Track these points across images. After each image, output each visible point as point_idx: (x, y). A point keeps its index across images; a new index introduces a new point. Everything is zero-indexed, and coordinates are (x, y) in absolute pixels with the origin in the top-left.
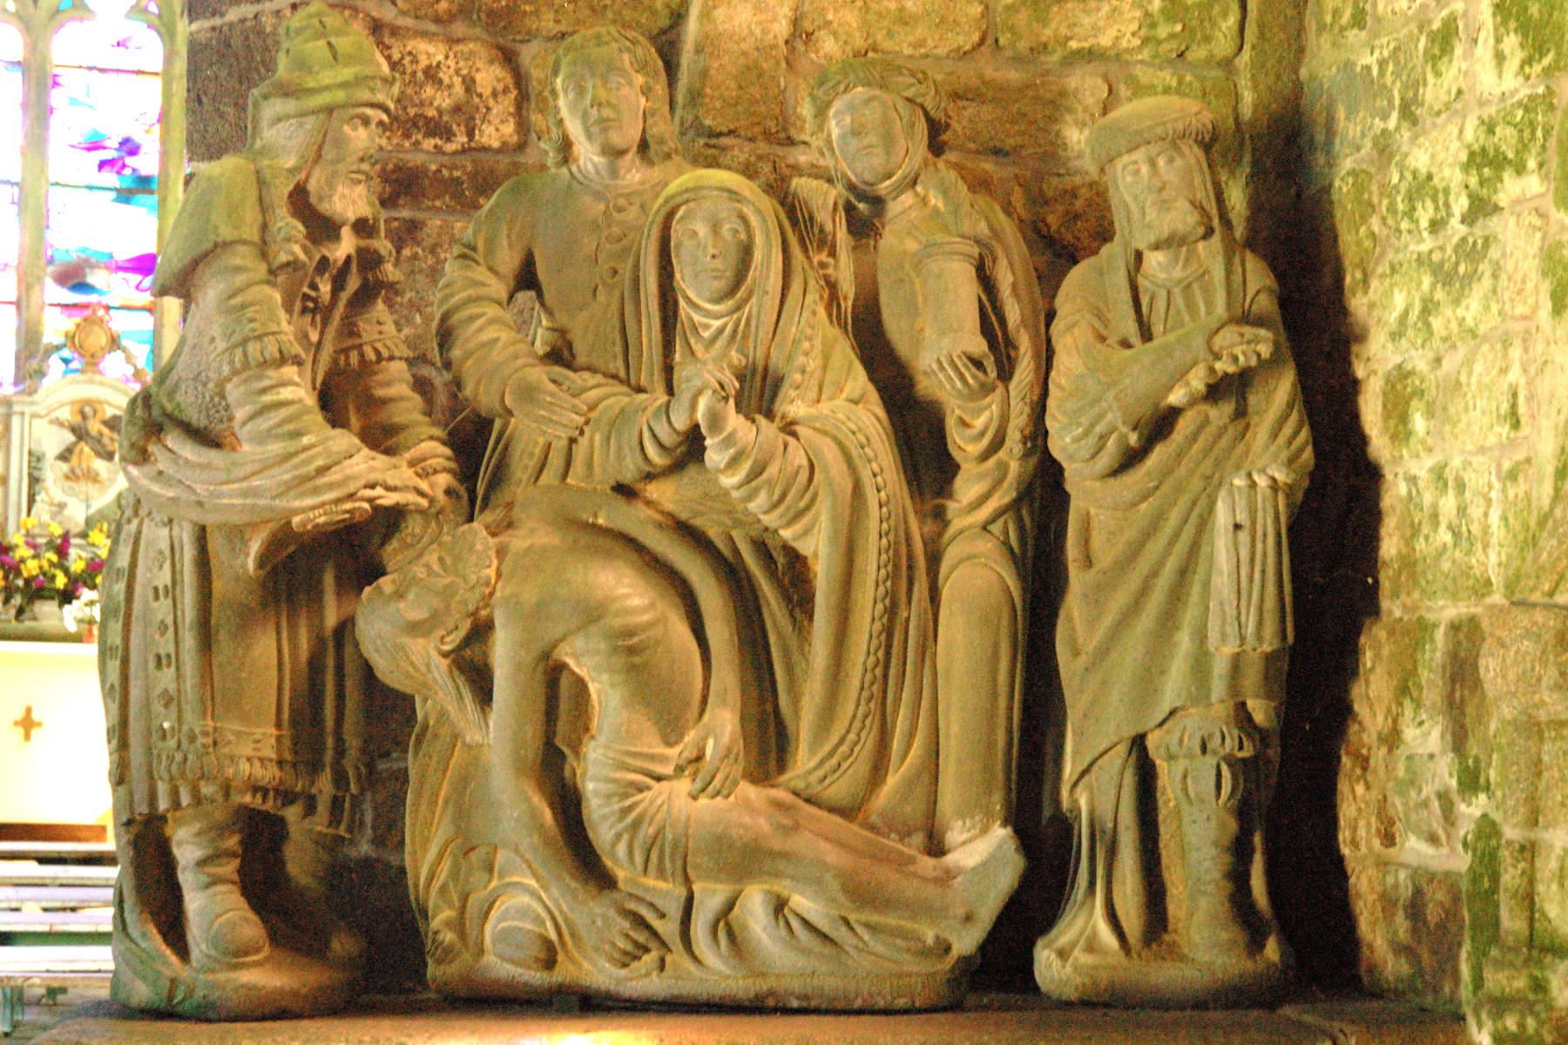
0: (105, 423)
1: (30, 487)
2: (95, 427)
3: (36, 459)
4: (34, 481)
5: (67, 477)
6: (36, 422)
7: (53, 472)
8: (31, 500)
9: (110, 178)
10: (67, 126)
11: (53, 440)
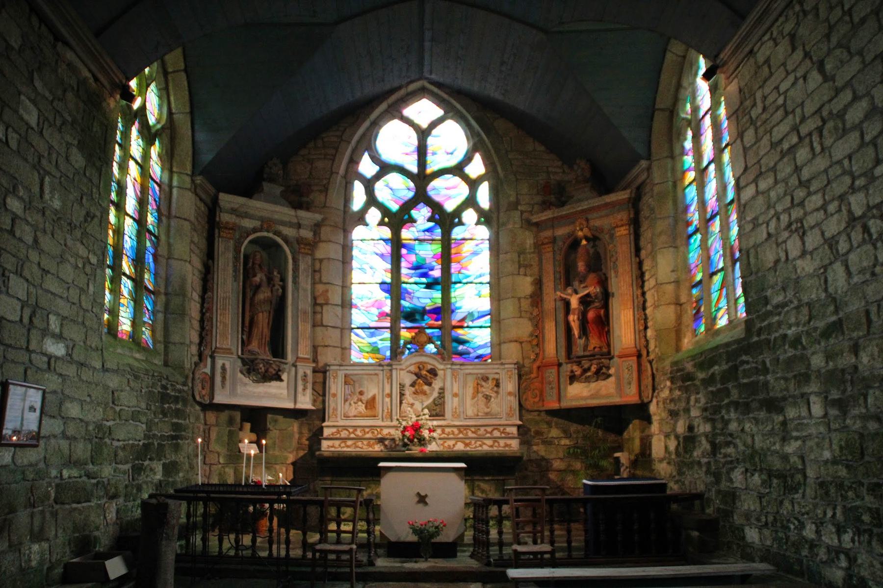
0: (428, 371)
1: (400, 397)
2: (424, 372)
3: (402, 386)
4: (402, 395)
5: (414, 393)
6: (402, 372)
7: (408, 391)
8: (401, 403)
9: (424, 280)
11: (408, 379)
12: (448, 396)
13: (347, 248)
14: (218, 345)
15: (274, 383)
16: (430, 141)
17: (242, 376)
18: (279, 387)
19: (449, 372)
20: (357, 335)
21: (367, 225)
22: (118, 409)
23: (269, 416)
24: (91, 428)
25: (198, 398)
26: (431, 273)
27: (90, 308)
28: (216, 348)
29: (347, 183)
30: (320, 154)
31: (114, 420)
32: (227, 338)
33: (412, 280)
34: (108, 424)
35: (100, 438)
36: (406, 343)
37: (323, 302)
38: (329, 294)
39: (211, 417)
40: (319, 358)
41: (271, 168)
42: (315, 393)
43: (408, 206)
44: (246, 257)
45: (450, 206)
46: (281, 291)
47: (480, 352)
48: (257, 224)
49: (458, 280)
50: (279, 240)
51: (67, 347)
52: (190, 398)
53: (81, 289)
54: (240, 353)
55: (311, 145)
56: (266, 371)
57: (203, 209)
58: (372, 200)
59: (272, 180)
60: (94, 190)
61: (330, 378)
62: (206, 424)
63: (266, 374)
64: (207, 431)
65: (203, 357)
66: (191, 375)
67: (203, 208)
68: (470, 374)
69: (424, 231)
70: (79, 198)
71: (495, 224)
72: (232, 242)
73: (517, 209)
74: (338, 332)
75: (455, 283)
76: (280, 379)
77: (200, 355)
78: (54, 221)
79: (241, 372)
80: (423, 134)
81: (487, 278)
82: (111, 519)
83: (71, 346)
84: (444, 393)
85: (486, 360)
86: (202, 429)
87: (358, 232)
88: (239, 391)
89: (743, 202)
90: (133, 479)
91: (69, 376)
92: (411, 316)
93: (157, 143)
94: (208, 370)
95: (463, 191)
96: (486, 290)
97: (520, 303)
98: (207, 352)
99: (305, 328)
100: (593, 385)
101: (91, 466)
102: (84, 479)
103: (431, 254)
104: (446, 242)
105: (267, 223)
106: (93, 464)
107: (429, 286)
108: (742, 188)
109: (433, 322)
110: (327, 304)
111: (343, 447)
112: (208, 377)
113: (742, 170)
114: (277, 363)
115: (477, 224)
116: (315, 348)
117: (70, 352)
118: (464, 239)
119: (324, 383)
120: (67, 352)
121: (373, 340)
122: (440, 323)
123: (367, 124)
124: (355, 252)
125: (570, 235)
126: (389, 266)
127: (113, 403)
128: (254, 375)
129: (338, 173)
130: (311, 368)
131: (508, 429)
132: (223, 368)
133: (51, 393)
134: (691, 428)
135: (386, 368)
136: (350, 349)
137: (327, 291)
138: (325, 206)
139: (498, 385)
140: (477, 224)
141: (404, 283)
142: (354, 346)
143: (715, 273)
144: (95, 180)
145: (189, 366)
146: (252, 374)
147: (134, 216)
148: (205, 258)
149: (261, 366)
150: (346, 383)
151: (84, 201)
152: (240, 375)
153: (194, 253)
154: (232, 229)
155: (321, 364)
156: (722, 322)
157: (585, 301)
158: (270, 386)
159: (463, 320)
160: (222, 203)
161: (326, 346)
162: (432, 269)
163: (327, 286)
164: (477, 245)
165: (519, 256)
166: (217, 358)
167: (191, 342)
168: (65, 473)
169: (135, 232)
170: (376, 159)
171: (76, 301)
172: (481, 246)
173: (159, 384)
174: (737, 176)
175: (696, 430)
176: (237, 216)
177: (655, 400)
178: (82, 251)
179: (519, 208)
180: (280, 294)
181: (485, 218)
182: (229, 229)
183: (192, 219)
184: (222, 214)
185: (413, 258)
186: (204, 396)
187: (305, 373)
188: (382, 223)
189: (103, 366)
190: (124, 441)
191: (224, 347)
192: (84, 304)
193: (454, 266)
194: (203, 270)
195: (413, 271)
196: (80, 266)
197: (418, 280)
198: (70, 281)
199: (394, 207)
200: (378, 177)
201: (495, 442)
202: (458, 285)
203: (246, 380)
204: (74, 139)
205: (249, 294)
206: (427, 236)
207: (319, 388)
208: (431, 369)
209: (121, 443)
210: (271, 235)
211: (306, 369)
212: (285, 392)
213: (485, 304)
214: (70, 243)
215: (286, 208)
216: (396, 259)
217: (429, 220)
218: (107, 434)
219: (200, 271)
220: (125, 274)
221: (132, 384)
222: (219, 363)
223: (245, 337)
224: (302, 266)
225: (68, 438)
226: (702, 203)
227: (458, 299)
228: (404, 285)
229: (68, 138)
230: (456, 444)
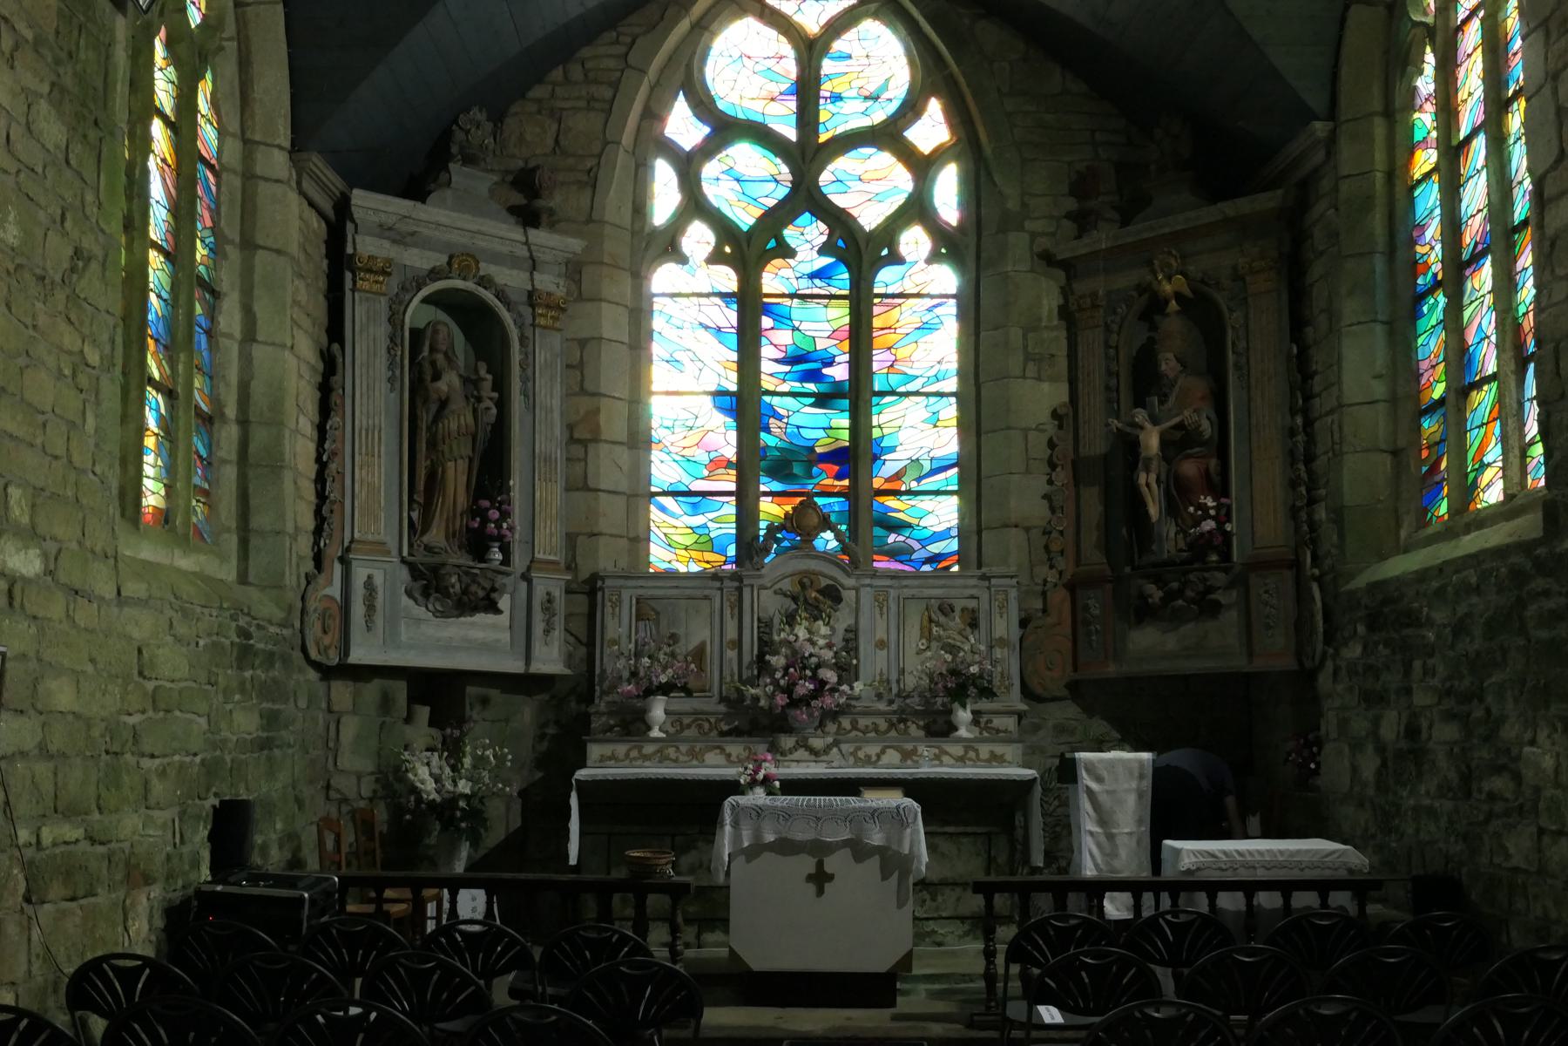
0: (819, 591)
6: (764, 592)
9: (811, 387)
10: (775, 342)
12: (865, 646)
13: (639, 315)
14: (357, 535)
15: (480, 618)
16: (827, 66)
17: (411, 603)
18: (494, 627)
19: (867, 596)
20: (663, 509)
21: (683, 260)
22: (150, 686)
23: (472, 691)
24: (96, 733)
25: (314, 654)
26: (826, 371)
27: (89, 466)
28: (352, 541)
29: (637, 166)
30: (579, 98)
31: (143, 712)
33: (785, 388)
34: (131, 720)
35: (116, 754)
36: (771, 529)
37: (588, 436)
38: (602, 418)
39: (342, 692)
40: (578, 559)
41: (467, 132)
42: (571, 639)
43: (776, 218)
44: (416, 334)
45: (870, 218)
46: (494, 411)
47: (935, 548)
48: (441, 260)
49: (888, 389)
50: (488, 296)
51: (45, 556)
52: (297, 655)
53: (72, 425)
54: (405, 553)
55: (557, 74)
56: (465, 591)
57: (316, 225)
58: (695, 204)
59: (469, 160)
60: (90, 198)
62: (330, 711)
63: (465, 598)
65: (326, 564)
66: (299, 605)
67: (317, 224)
68: (913, 597)
69: (812, 276)
70: (58, 219)
71: (972, 265)
72: (383, 300)
73: (1021, 228)
74: (620, 502)
75: (882, 394)
76: (492, 608)
77: (318, 559)
78: (8, 272)
79: (409, 594)
80: (811, 50)
81: (951, 385)
82: (138, 932)
83: (54, 552)
84: (856, 639)
85: (948, 568)
86: (321, 721)
87: (664, 277)
88: (404, 638)
89: (1550, 232)
90: (182, 841)
91: (50, 620)
92: (782, 467)
93: (209, 76)
94: (335, 591)
95: (902, 182)
96: (949, 410)
97: (1026, 438)
98: (333, 551)
99: (551, 495)
100: (1188, 629)
101: (96, 816)
102: (84, 846)
103: (827, 328)
104: (861, 302)
105: (462, 261)
106: (101, 813)
107: (822, 400)
108: (1551, 200)
109: (829, 482)
111: (635, 759)
113: (1551, 160)
114: (490, 574)
115: (929, 261)
116: (571, 539)
117: (52, 567)
118: (901, 295)
119: (591, 616)
120: (46, 566)
121: (698, 520)
122: (846, 482)
123: (684, 25)
124: (657, 323)
125: (1142, 289)
126: (734, 357)
127: (141, 673)
128: (437, 599)
129: (619, 143)
130: (563, 583)
131: (998, 722)
132: (369, 585)
133: (16, 658)
134: (1412, 732)
135: (727, 583)
136: (648, 540)
137: (597, 411)
138: (590, 220)
139: (974, 625)
140: (929, 261)
141: (768, 393)
142: (656, 534)
143: (1477, 386)
144: (90, 175)
145: (294, 583)
146: (432, 599)
147: (164, 244)
148: (324, 339)
149: (454, 579)
150: (639, 618)
151: (68, 224)
152: (405, 601)
153: (299, 327)
154: (384, 273)
155: (584, 574)
156: (1492, 493)
157: (1178, 442)
158: (473, 624)
159: (898, 476)
160: (357, 213)
161: (595, 535)
162: (830, 363)
164: (930, 310)
165: (1025, 337)
166: (354, 563)
167: (296, 528)
168: (47, 836)
169: (167, 285)
170: (704, 106)
171: (60, 450)
172: (938, 311)
173: (234, 624)
174: (1540, 171)
175: (1424, 735)
176: (394, 241)
177: (1329, 665)
178: (70, 340)
179: (1028, 225)
180: (493, 419)
181: (948, 245)
182: (376, 273)
183: (294, 249)
184: (359, 239)
185: (784, 337)
186: (327, 648)
187: (548, 594)
188: (716, 258)
189: (119, 593)
190: (165, 756)
191: (370, 537)
192: (76, 458)
193: (879, 360)
194: (320, 366)
195: (787, 368)
196: (67, 372)
197: (797, 386)
198: (49, 408)
199: (745, 218)
200: (708, 149)
201: (967, 749)
202: (888, 399)
203: (420, 611)
204: (42, 81)
205: (425, 419)
206: (819, 287)
207: (580, 628)
208: (828, 586)
209: (157, 761)
210: (469, 285)
211: (549, 585)
212: (505, 637)
213: (947, 443)
214: (42, 320)
215: (504, 226)
216: (748, 341)
217: (823, 250)
218: (130, 743)
219: (313, 368)
220: (151, 381)
221: (181, 630)
222: (360, 574)
223: (415, 515)
224: (541, 357)
225: (51, 757)
226: (1453, 225)
227: (886, 431)
228: (767, 399)
229: (29, 80)
230: (883, 752)
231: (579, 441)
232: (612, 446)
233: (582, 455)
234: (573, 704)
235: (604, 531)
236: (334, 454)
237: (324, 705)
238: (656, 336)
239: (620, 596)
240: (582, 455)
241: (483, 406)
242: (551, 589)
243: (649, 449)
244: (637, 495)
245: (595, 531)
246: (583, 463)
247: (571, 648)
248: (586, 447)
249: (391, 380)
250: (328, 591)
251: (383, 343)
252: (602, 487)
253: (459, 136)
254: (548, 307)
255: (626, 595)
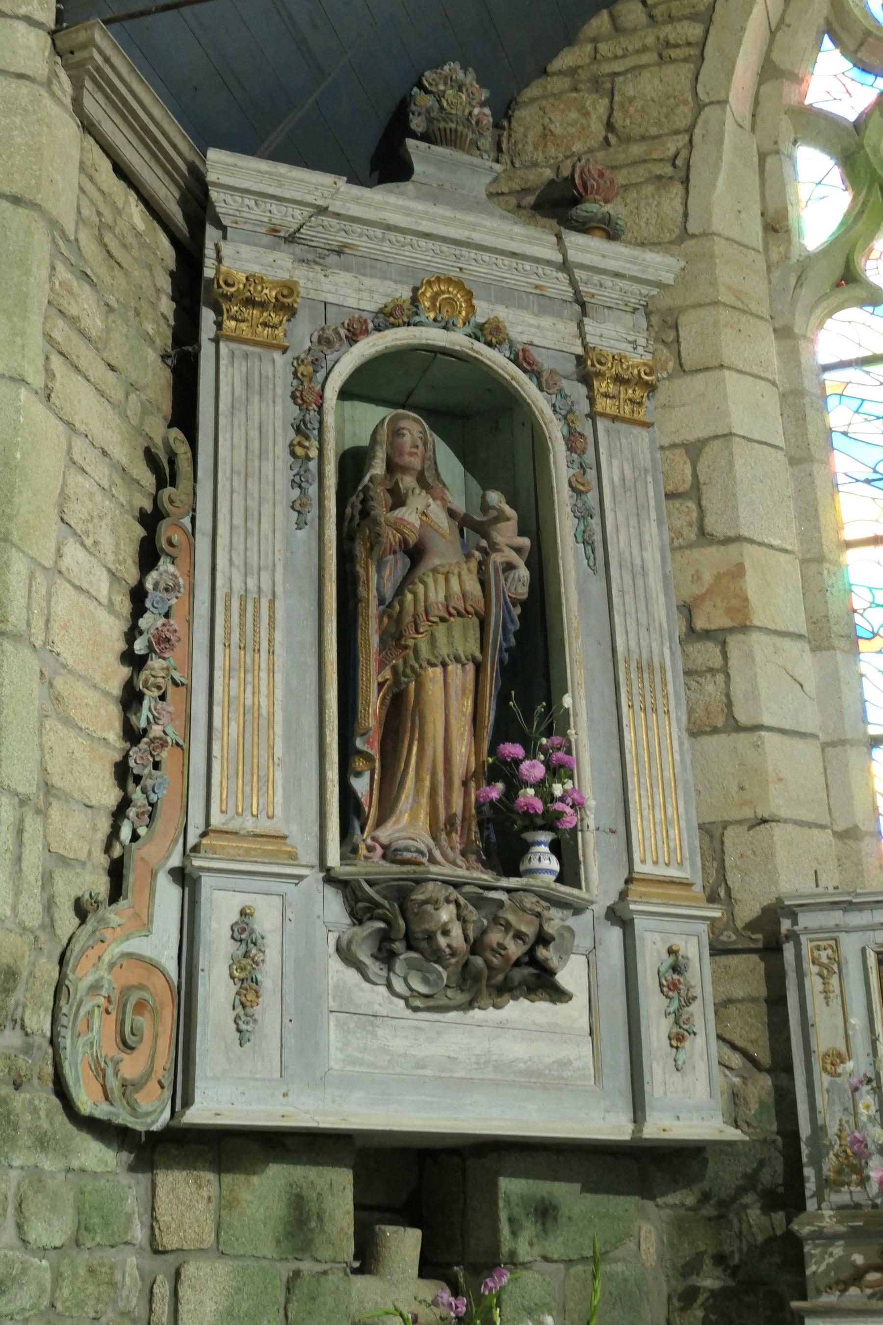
14: (216, 820)
17: (352, 975)
18: (552, 1031)
30: (645, 49)
32: (265, 782)
37: (721, 621)
38: (751, 584)
40: (734, 878)
42: (736, 1060)
46: (524, 573)
54: (334, 858)
55: (601, 22)
56: (476, 946)
61: (801, 975)
63: (479, 961)
64: (162, 1290)
65: (132, 879)
74: (809, 751)
79: (345, 953)
88: (335, 1057)
110: (744, 628)
112: (158, 984)
114: (530, 901)
128: (411, 965)
129: (724, 102)
130: (703, 928)
137: (739, 571)
138: (685, 234)
146: (399, 965)
149: (446, 914)
158: (501, 1026)
161: (764, 821)
163: (733, 548)
166: (207, 881)
180: (523, 592)
182: (262, 305)
184: (227, 249)
191: (249, 824)
231: (708, 635)
232: (778, 640)
233: (717, 661)
234: (754, 1214)
235: (783, 813)
236: (163, 641)
237: (139, 1234)
238: (838, 440)
239: (836, 948)
240: (717, 661)
241: (497, 558)
242: (679, 943)
243: (855, 651)
244: (843, 742)
245: (766, 815)
246: (720, 678)
247: (736, 1080)
248: (724, 643)
249: (298, 508)
250: (137, 945)
251: (284, 436)
252: (767, 721)
253: (424, 101)
254: (618, 380)
255: (850, 945)
